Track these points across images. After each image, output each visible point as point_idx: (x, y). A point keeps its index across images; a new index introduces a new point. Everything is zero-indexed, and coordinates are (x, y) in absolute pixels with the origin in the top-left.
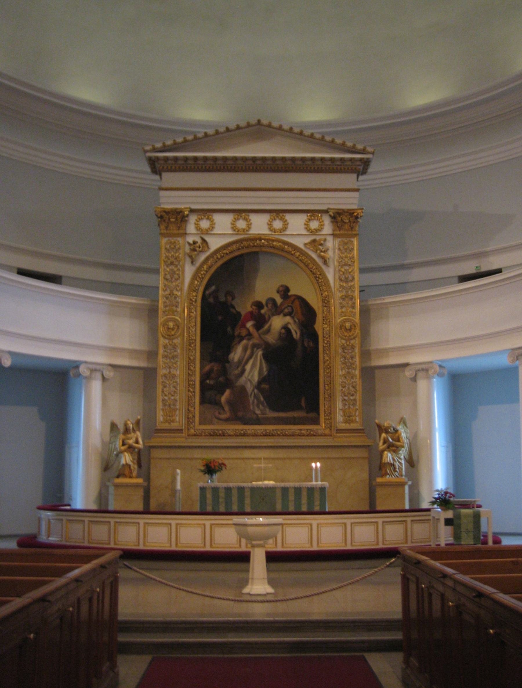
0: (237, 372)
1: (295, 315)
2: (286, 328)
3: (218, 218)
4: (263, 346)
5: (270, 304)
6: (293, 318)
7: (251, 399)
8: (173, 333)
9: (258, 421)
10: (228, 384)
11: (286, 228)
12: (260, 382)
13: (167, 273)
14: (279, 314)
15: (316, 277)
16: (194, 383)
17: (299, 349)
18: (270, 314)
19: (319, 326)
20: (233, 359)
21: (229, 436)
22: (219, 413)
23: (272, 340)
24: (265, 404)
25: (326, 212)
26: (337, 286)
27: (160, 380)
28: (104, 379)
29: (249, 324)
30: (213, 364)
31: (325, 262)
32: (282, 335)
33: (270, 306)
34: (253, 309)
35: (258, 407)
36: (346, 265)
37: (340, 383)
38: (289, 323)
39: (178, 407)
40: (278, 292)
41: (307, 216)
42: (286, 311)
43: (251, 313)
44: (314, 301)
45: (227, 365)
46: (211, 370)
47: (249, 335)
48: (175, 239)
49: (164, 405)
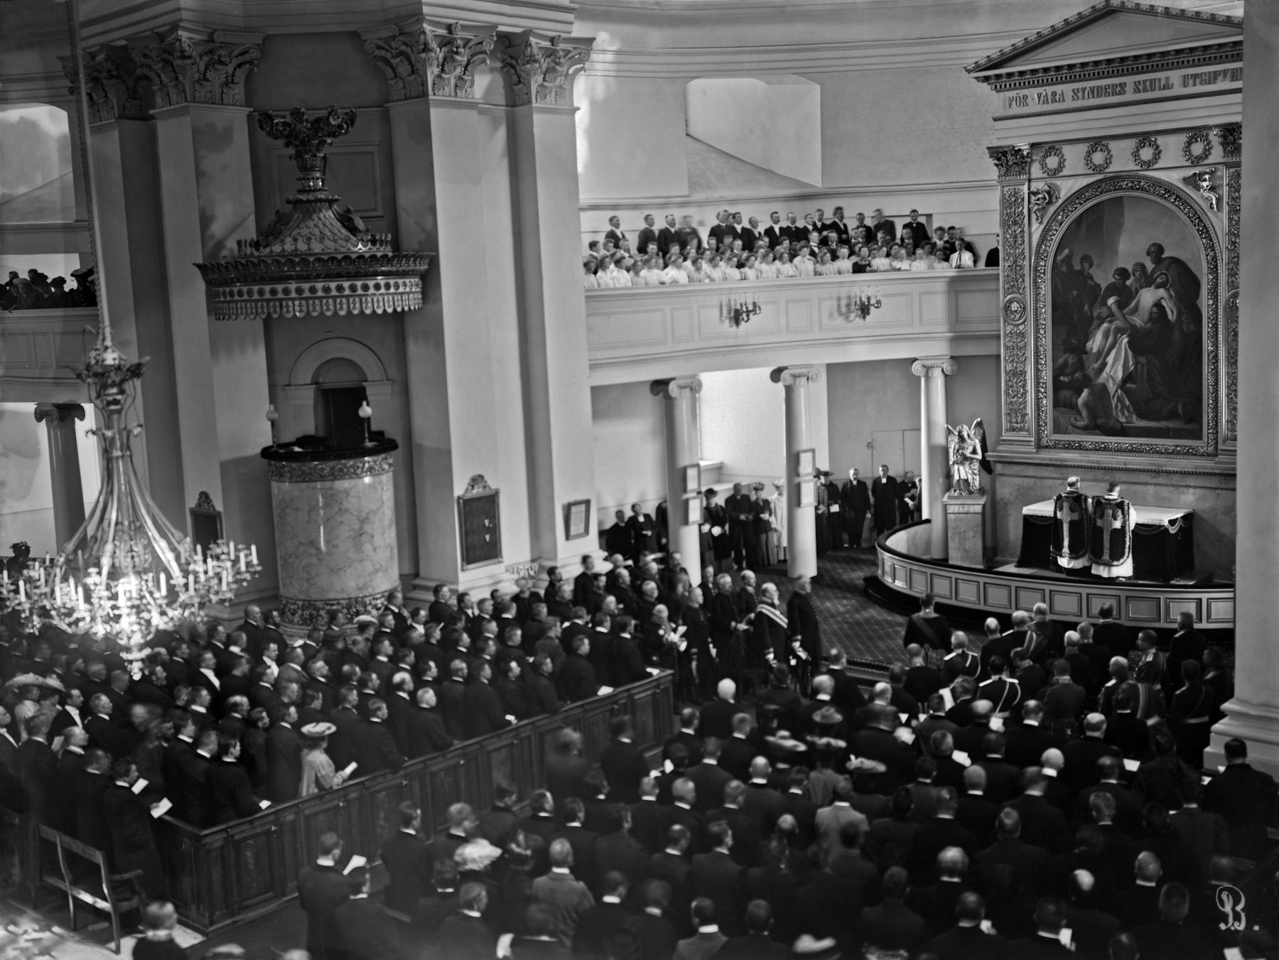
0: (1096, 366)
2: (1158, 305)
6: (1168, 290)
7: (1114, 402)
9: (1123, 431)
17: (1176, 335)
20: (1092, 349)
21: (1087, 450)
30: (1066, 356)
35: (1123, 414)
40: (1148, 254)
42: (1159, 280)
45: (1084, 356)
46: (1065, 363)
47: (1111, 315)
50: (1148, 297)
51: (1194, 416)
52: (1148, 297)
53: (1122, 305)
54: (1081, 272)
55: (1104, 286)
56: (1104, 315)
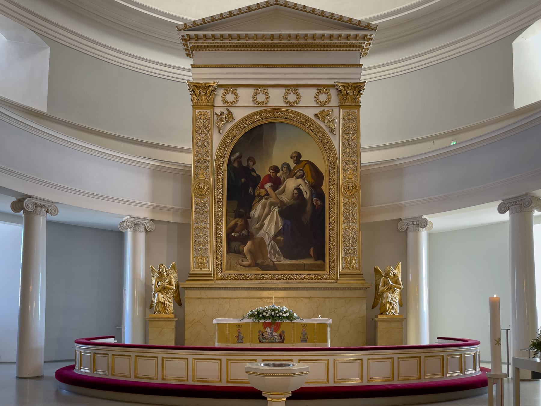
0: (257, 226)
1: (305, 177)
2: (298, 189)
3: (241, 92)
4: (279, 204)
5: (285, 168)
6: (304, 180)
8: (203, 193)
9: (274, 268)
10: (249, 236)
11: (299, 101)
12: (276, 236)
13: (198, 141)
14: (293, 177)
15: (324, 145)
16: (221, 236)
17: (309, 207)
18: (285, 177)
19: (325, 188)
20: (254, 215)
22: (243, 261)
23: (287, 199)
24: (280, 253)
25: (334, 86)
26: (342, 152)
27: (192, 232)
28: (146, 231)
29: (268, 186)
30: (236, 220)
31: (331, 131)
32: (294, 195)
33: (285, 170)
34: (271, 173)
35: (275, 256)
36: (350, 133)
37: (343, 235)
38: (300, 185)
39: (208, 256)
40: (291, 158)
41: (317, 90)
42: (298, 174)
43: (269, 175)
44: (322, 166)
46: (236, 225)
47: (267, 194)
48: (205, 111)
49: (197, 253)
50: (291, 184)
51: (321, 255)
52: (291, 184)
53: (275, 187)
54: (247, 168)
55: (262, 177)
56: (263, 194)
